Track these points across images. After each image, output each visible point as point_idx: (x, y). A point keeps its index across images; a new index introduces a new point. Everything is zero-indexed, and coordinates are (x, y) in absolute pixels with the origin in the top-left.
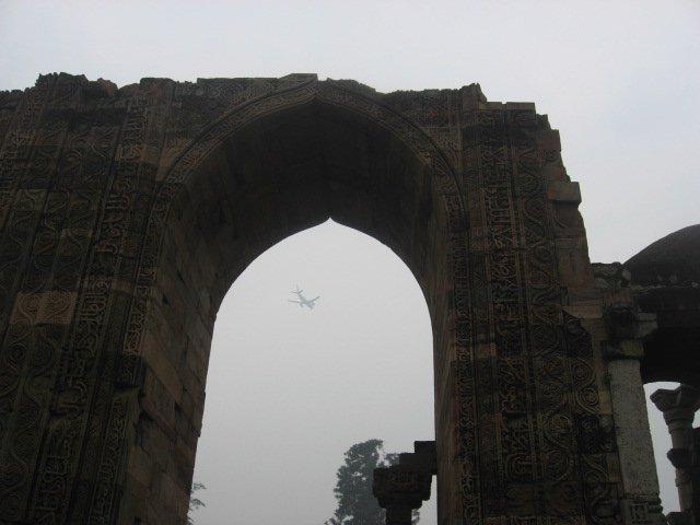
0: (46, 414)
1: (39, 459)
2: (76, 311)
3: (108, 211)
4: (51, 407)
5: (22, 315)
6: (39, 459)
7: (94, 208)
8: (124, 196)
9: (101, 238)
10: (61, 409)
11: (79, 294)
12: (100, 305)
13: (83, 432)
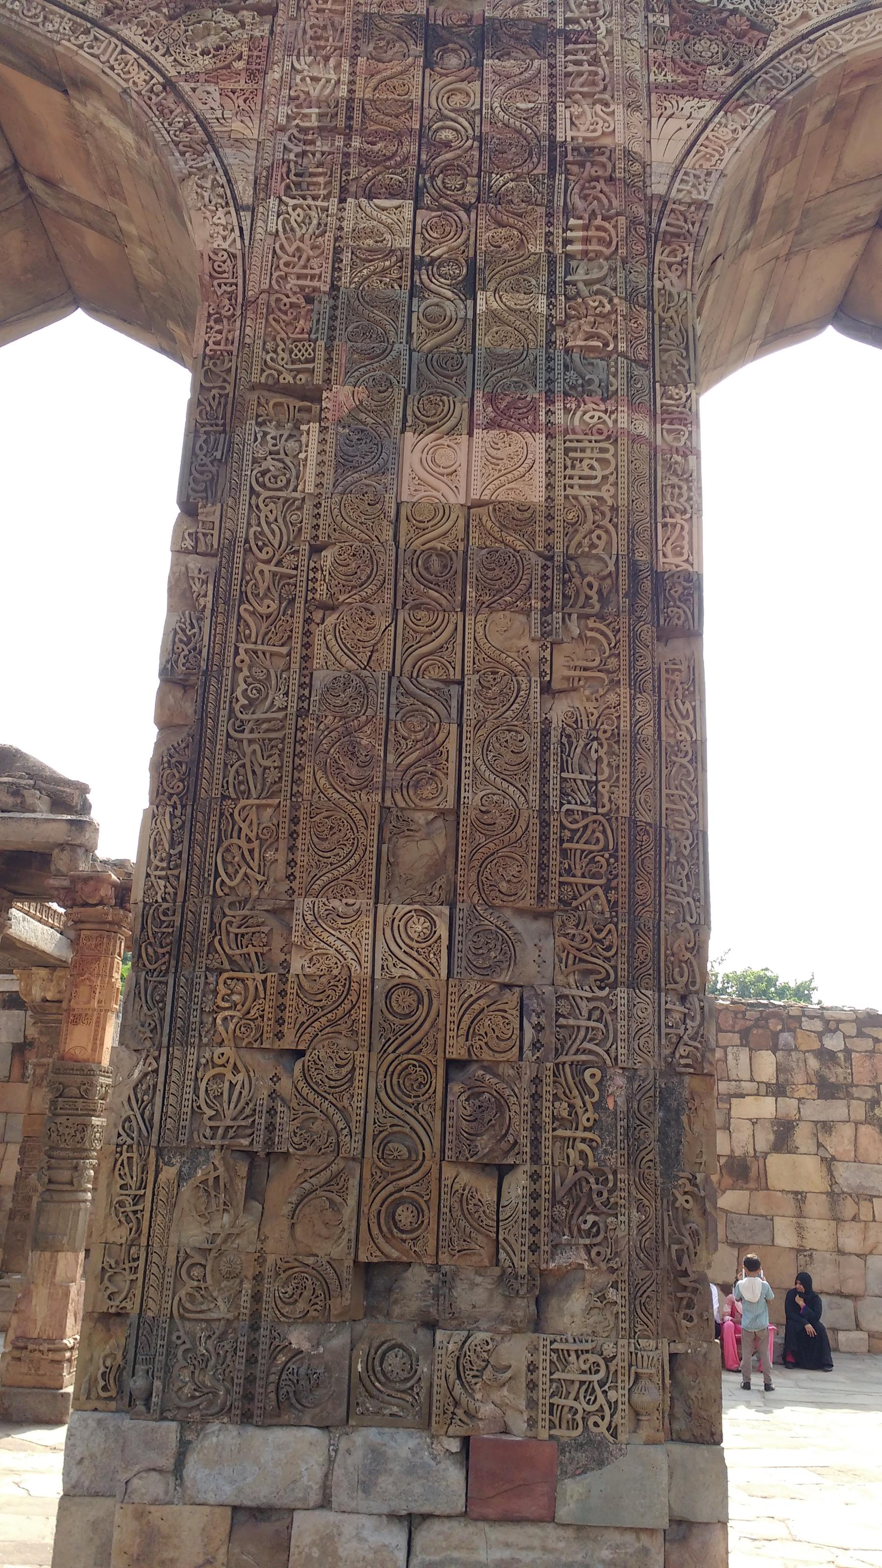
0: (536, 690)
4: (542, 674)
5: (422, 482)
7: (537, 247)
8: (598, 221)
10: (567, 679)
12: (604, 462)
13: (625, 726)
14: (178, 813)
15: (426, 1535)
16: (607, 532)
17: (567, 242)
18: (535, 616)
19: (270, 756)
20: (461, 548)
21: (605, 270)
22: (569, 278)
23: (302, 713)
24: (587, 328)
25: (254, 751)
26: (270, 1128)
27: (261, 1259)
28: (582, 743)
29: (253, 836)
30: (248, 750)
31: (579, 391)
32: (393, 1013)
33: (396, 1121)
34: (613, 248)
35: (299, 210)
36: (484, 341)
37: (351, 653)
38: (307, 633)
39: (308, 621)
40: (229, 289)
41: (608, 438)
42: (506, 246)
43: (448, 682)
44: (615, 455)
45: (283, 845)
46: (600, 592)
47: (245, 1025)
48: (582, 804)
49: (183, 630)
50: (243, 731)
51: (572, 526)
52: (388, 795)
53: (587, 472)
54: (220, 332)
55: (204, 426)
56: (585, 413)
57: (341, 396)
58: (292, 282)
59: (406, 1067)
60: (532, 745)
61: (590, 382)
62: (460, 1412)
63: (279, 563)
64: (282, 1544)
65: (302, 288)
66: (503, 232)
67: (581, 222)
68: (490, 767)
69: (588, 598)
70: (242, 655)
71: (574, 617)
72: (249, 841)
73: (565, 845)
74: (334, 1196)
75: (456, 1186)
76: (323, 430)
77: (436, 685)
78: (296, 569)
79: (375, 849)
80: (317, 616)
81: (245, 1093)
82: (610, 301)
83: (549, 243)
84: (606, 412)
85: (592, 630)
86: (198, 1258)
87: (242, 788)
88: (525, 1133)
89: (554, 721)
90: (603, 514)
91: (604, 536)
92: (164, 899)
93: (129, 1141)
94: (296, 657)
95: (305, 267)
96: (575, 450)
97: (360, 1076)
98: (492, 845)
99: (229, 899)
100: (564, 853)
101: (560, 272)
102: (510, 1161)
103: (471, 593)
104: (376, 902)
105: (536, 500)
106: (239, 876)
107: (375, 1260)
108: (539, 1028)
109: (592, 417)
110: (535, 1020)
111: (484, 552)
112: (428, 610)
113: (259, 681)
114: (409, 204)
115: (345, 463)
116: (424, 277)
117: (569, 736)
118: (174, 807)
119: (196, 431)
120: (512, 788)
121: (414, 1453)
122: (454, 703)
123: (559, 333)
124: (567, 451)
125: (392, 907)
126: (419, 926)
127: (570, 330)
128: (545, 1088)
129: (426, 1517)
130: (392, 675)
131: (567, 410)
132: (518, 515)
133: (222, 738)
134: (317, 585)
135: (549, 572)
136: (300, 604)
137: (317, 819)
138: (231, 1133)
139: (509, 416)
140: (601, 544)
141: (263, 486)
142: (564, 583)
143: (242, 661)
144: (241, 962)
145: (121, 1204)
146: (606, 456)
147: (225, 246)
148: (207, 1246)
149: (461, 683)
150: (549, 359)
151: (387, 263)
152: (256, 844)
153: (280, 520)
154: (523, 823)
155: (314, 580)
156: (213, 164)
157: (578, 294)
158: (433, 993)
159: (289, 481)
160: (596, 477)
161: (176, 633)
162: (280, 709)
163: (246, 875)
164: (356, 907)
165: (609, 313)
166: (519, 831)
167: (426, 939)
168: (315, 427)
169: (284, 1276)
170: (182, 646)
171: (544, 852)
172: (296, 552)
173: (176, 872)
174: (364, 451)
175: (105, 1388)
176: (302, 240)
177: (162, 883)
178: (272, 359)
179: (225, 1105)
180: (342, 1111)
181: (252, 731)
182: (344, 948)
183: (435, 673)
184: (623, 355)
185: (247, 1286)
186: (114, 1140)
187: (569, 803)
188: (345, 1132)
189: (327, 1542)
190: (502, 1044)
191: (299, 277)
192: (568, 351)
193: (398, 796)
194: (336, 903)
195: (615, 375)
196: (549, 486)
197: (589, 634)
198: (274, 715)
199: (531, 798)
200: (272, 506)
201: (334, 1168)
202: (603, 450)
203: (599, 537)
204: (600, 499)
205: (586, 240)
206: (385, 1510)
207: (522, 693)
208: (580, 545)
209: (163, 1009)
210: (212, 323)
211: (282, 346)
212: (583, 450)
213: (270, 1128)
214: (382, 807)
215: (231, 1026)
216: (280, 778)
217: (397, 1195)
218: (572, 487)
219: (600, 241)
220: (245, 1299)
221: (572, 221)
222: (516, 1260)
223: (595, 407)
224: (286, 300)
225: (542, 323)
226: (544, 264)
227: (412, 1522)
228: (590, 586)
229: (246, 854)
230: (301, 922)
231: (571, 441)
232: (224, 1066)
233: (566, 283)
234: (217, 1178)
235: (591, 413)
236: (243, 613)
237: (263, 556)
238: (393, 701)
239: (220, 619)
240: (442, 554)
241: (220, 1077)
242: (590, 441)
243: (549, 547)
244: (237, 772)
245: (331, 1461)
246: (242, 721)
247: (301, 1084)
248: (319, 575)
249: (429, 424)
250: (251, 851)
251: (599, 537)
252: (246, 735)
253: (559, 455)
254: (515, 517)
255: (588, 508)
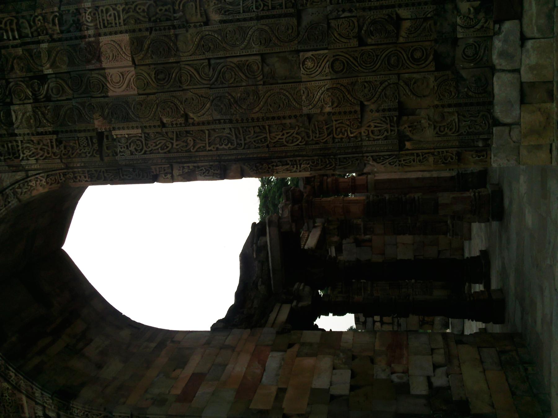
0: (208, 28)
1: (245, 20)
2: (116, 33)
3: (21, 37)
4: (201, 26)
5: (128, 85)
6: (245, 20)
7: (20, 51)
9: (47, 34)
10: (201, 16)
11: (100, 35)
12: (107, 11)
14: (275, 164)
15: (528, 33)
16: (136, 6)
17: (14, 38)
18: (178, 31)
19: (249, 132)
20: (152, 66)
21: (24, 20)
22: (30, 35)
23: (231, 121)
24: (51, 25)
25: (249, 138)
26: (389, 110)
27: (437, 106)
28: (227, 6)
29: (281, 134)
30: (248, 140)
31: (78, 25)
32: (343, 69)
33: (383, 63)
34: (13, 18)
35: (25, 152)
36: (64, 68)
37: (204, 105)
38: (198, 124)
39: (193, 124)
40: (62, 175)
41: (96, 10)
42: (22, 65)
43: (209, 64)
44: (103, 6)
45: (284, 121)
46: (163, 6)
47: (353, 125)
48: (252, 3)
49: (204, 173)
50: (241, 144)
51: (138, 21)
52: (259, 83)
53: (113, 17)
54: (80, 177)
55: (120, 177)
56: (87, 22)
57: (98, 124)
58: (55, 150)
59: (363, 62)
60: (230, 27)
61: (74, 21)
62: (485, 25)
63: (172, 139)
64: (532, 85)
65: (57, 146)
66: (16, 66)
67: (5, 34)
68: (242, 43)
69: (166, 10)
70: (211, 148)
71: (175, 15)
72: (283, 135)
73: (270, 8)
74: (412, 83)
75: (406, 36)
76: (114, 129)
77: (211, 70)
78: (173, 132)
79: (281, 85)
80: (190, 121)
81: (377, 121)
82: (37, 16)
83: (16, 46)
84: (85, 13)
85: (179, 8)
86: (437, 129)
87: (263, 140)
88: (384, 12)
89: (219, 18)
90: (129, 8)
91: (139, 7)
92: (308, 164)
93: (398, 162)
94: (209, 127)
95: (48, 146)
96: (104, 24)
97: (368, 79)
98: (274, 39)
99: (306, 139)
100: (273, 8)
101: (28, 40)
102: (394, 16)
103: (172, 60)
104: (301, 82)
105: (128, 37)
106: (298, 136)
107: (434, 64)
108: (344, 11)
109: (89, 18)
110: (341, 13)
111: (154, 57)
112: (181, 77)
113: (220, 140)
114: (12, 108)
115: (126, 118)
116: (41, 97)
117: (225, 12)
118: (273, 166)
119: (123, 180)
120: (250, 33)
121: (500, 41)
122: (218, 61)
123: (55, 36)
124: (105, 27)
125: (302, 76)
126: (309, 64)
127: (52, 32)
128: (367, 5)
129: (522, 33)
130: (210, 88)
131: (88, 29)
132: (136, 44)
133: (245, 151)
134: (179, 123)
135: (158, 28)
136: (188, 129)
137: (272, 110)
138: (392, 124)
139: (94, 53)
140: (142, 7)
141: (141, 150)
142: (161, 21)
143: (214, 148)
144: (330, 130)
145: (420, 161)
146: (104, 10)
147: (44, 180)
148: (433, 127)
149: (209, 60)
150: (66, 39)
151: (39, 113)
152: (284, 132)
153: (155, 141)
154: (263, 27)
155: (176, 124)
156: (11, 190)
157: (36, 30)
158: (334, 54)
159: (138, 140)
160: (114, 14)
161: (205, 176)
162: (231, 130)
163: (297, 134)
164: (304, 89)
165: (42, 16)
166: (267, 28)
167: (313, 60)
168: (114, 133)
169: (442, 97)
170: (210, 173)
171: (274, 17)
172: (167, 133)
173: (298, 161)
174: (121, 111)
175: (483, 156)
176: (37, 149)
177: (302, 166)
178: (89, 153)
179: (382, 128)
180: (381, 84)
181: (241, 140)
182: (321, 92)
183: (206, 70)
184: (59, 8)
185: (446, 110)
186: (397, 167)
187: (253, 8)
188: (389, 81)
189: (532, 68)
190: (351, 24)
191: (52, 147)
192: (62, 32)
193: (259, 79)
194: (304, 97)
195: (69, 11)
196: (121, 32)
197: (181, 8)
198: (233, 132)
199: (252, 24)
200: (149, 145)
201: (402, 84)
202: (102, 11)
203: (140, 9)
204: (123, 10)
205: (12, 30)
206: (519, 49)
207: (210, 33)
208: (144, 17)
209: (349, 158)
210: (77, 180)
211: (83, 150)
212: (103, 20)
213: (389, 110)
214: (264, 84)
215: (354, 130)
216: (258, 126)
217: (410, 59)
218: (120, 23)
219: (11, 24)
220: (451, 110)
221: (5, 37)
222: (430, 10)
223: (84, 18)
224: (63, 152)
225: (52, 44)
226: (26, 47)
227: (523, 39)
228: (161, 10)
229: (289, 135)
230: (312, 110)
231: (100, 26)
232: (368, 131)
233: (33, 36)
234: (409, 127)
235: (87, 18)
236: (195, 149)
237: (170, 146)
238: (221, 86)
239: (198, 159)
240: (157, 74)
241: (373, 132)
242: (99, 18)
243: (147, 29)
244: (257, 143)
245: (503, 71)
246: (237, 144)
247: (373, 101)
248: (174, 123)
249: (103, 86)
250: (287, 133)
251: (140, 9)
252: (243, 142)
253: (106, 30)
254: (137, 45)
255: (128, 15)
